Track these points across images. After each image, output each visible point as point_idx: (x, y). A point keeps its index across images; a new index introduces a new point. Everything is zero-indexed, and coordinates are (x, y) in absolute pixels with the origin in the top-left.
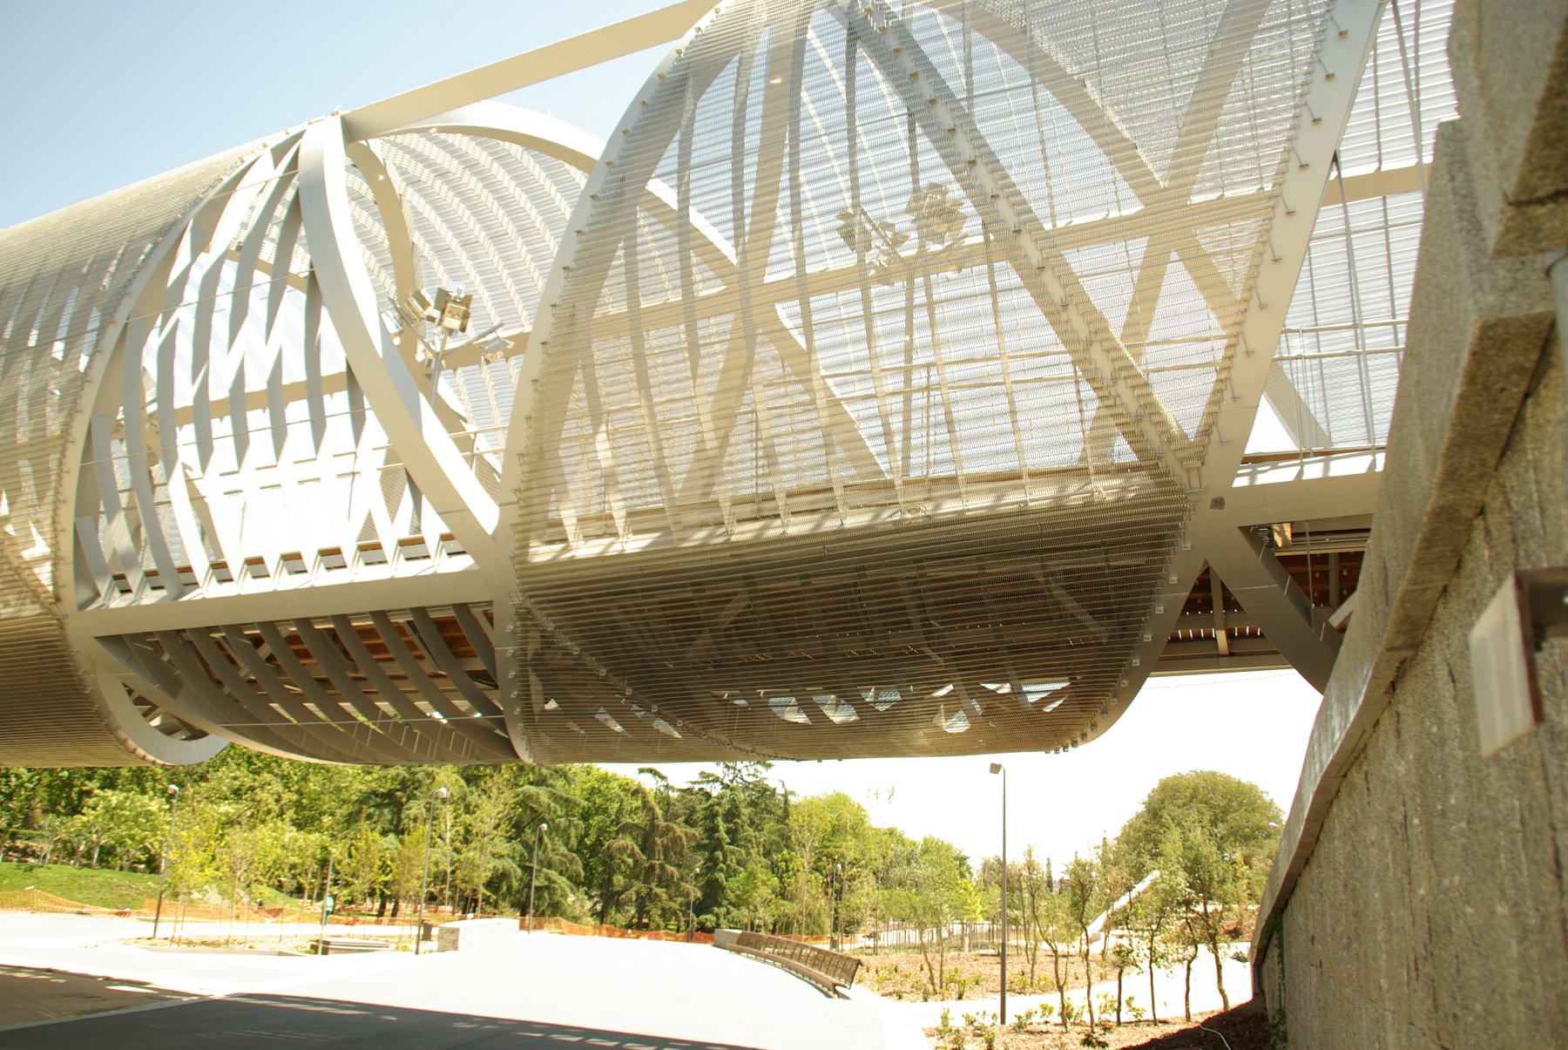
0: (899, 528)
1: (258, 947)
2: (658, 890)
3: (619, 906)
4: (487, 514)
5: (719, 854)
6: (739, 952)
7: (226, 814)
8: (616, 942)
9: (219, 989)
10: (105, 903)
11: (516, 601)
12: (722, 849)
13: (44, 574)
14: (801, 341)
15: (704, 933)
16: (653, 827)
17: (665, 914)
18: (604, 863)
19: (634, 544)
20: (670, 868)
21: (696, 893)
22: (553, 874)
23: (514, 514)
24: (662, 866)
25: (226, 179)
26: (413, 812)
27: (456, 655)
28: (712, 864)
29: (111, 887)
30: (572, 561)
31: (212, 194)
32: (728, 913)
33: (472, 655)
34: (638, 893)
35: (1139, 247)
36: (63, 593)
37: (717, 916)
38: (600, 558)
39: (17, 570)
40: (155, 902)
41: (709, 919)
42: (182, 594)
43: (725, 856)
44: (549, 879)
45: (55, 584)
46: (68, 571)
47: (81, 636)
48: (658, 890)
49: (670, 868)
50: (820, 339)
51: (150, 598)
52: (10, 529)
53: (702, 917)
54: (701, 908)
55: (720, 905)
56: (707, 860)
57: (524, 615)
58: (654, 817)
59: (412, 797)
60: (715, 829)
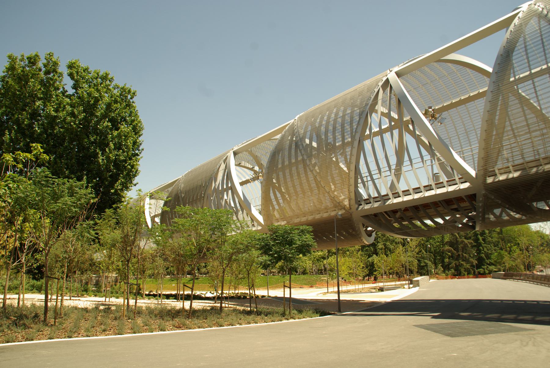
1: (362, 291)
2: (462, 262)
3: (449, 269)
4: (473, 173)
6: (505, 279)
7: (320, 255)
8: (449, 281)
9: (389, 300)
10: (306, 285)
11: (483, 192)
12: (482, 246)
13: (346, 203)
14: (538, 108)
15: (482, 275)
16: (457, 241)
18: (440, 255)
19: (516, 174)
20: (464, 255)
21: (475, 262)
22: (426, 261)
23: (482, 172)
24: (462, 255)
25: (373, 97)
26: (380, 247)
27: (448, 205)
28: (479, 252)
29: (306, 280)
30: (499, 181)
31: (371, 102)
32: (488, 267)
33: (454, 204)
34: (455, 264)
36: (352, 207)
37: (484, 269)
38: (507, 180)
39: (339, 203)
40: (335, 281)
41: (481, 270)
42: (385, 203)
43: (483, 248)
44: (425, 263)
46: (353, 202)
47: (356, 217)
48: (462, 262)
49: (464, 255)
50: (541, 102)
51: (376, 205)
52: (336, 193)
53: (479, 270)
54: (478, 267)
55: (484, 265)
56: (477, 250)
57: (485, 196)
58: (457, 238)
59: (378, 242)
60: (478, 239)
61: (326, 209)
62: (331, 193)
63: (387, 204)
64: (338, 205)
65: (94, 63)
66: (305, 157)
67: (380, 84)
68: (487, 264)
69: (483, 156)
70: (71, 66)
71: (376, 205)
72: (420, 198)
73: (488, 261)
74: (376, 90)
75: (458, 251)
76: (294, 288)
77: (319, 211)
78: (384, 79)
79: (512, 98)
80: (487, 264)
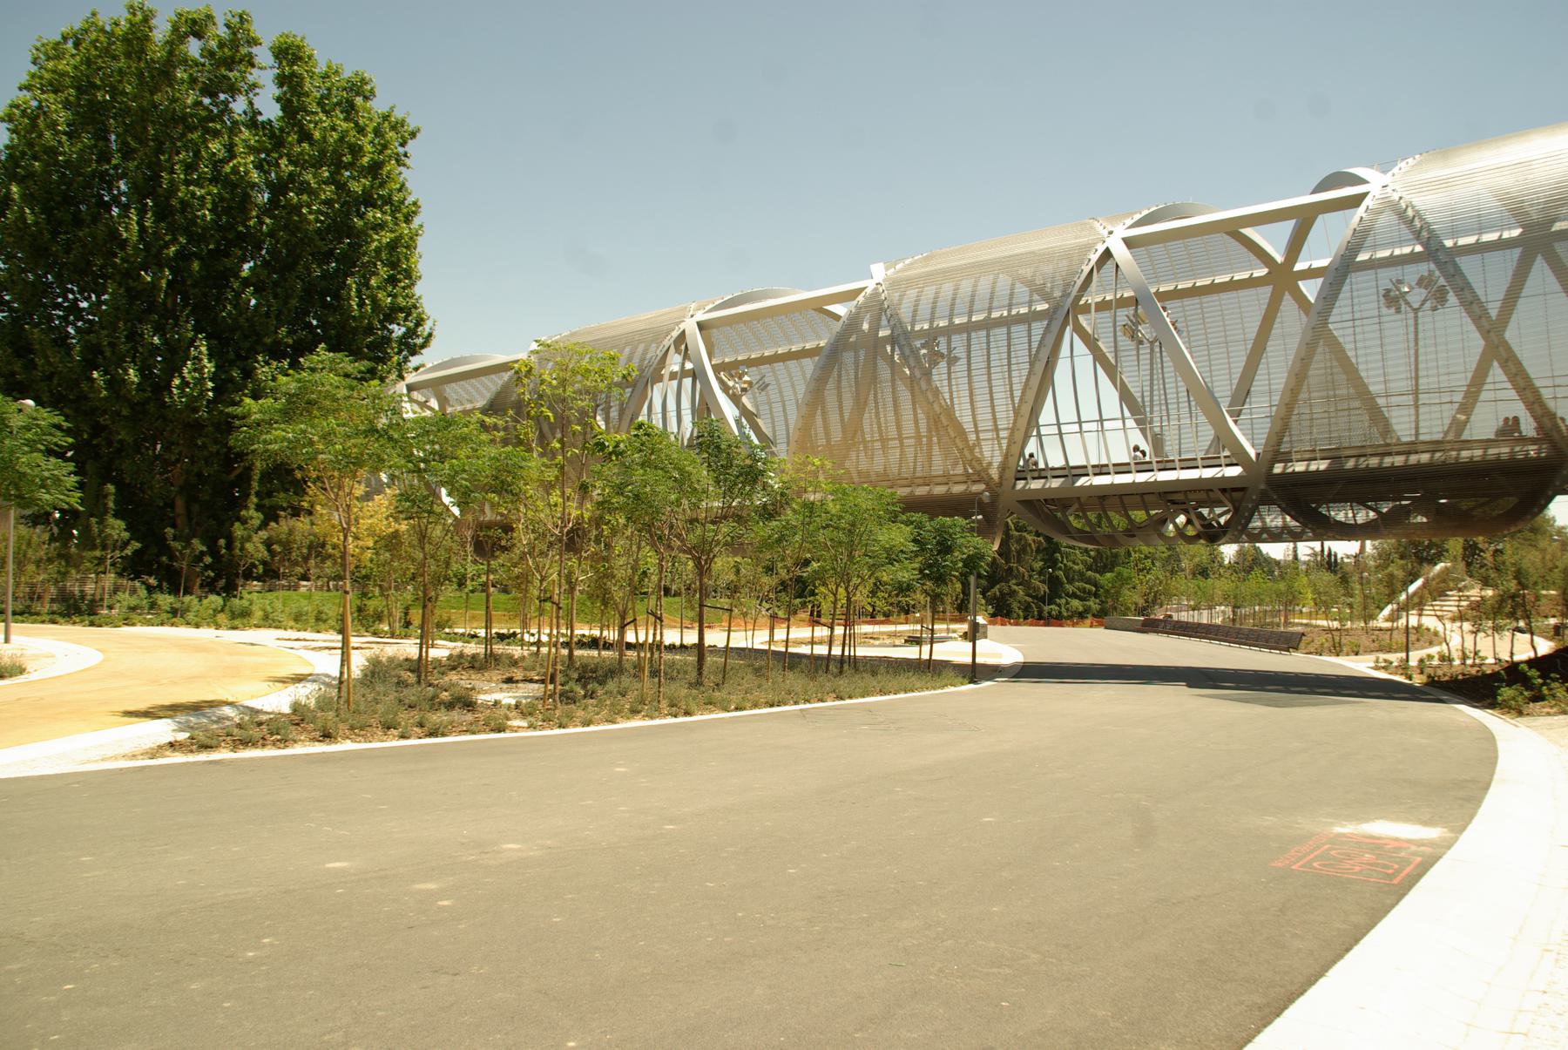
0: (1444, 463)
4: (1252, 453)
5: (1058, 555)
13: (994, 473)
17: (1027, 609)
19: (1323, 465)
21: (1044, 588)
23: (1269, 456)
25: (1079, 283)
28: (1052, 563)
30: (1293, 472)
35: (1517, 252)
38: (1306, 473)
51: (1056, 483)
61: (947, 479)
62: (966, 452)
63: (1078, 484)
64: (981, 476)
65: (334, 52)
66: (918, 373)
67: (1094, 257)
68: (1068, 595)
69: (1277, 429)
70: (288, 53)
71: (1056, 483)
72: (1146, 483)
73: (1070, 588)
74: (1087, 269)
78: (1101, 249)
79: (1287, 296)
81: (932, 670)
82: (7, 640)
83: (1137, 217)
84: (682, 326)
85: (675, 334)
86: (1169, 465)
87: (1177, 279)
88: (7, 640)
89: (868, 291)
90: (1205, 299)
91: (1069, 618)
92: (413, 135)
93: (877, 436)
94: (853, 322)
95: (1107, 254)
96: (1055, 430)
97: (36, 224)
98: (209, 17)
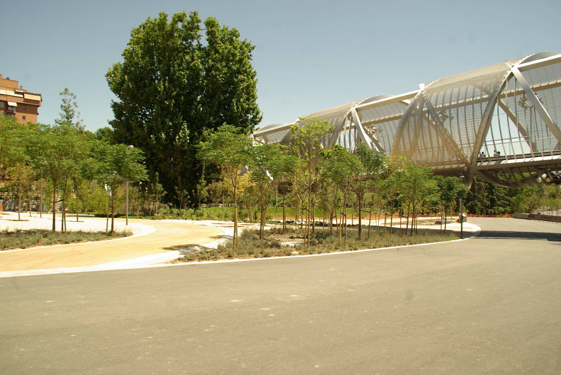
5: (494, 190)
13: (468, 160)
17: (482, 211)
21: (488, 203)
25: (501, 86)
28: (492, 193)
37: (494, 209)
45: (471, 161)
51: (493, 163)
55: (495, 206)
61: (450, 163)
62: (457, 152)
64: (463, 161)
65: (225, 23)
66: (438, 124)
67: (506, 76)
68: (498, 205)
70: (210, 24)
71: (493, 163)
72: (529, 162)
73: (499, 203)
74: (503, 81)
75: (474, 193)
76: (363, 218)
77: (443, 163)
78: (509, 72)
80: (498, 205)
81: (446, 234)
82: (127, 224)
83: (524, 59)
84: (350, 110)
85: (348, 113)
86: (512, 157)
87: (541, 82)
88: (127, 224)
89: (419, 94)
90: (553, 89)
91: (499, 214)
92: (253, 48)
93: (423, 148)
94: (413, 105)
95: (512, 75)
96: (492, 143)
97: (133, 87)
98: (184, 14)
